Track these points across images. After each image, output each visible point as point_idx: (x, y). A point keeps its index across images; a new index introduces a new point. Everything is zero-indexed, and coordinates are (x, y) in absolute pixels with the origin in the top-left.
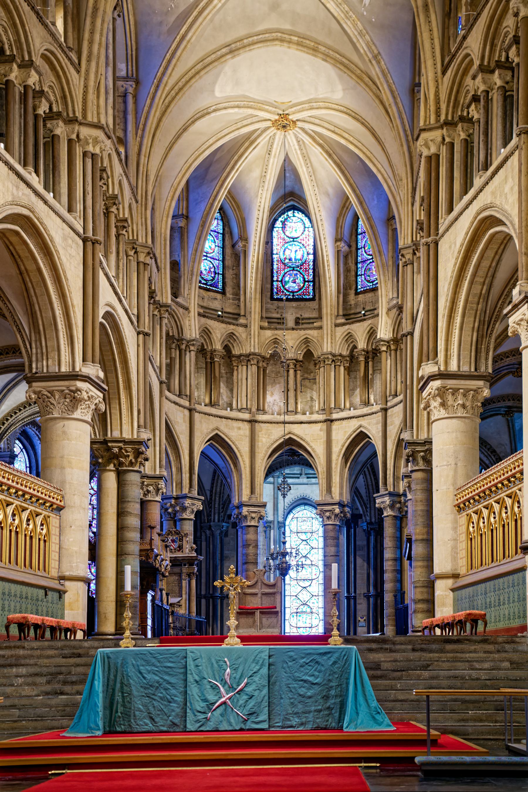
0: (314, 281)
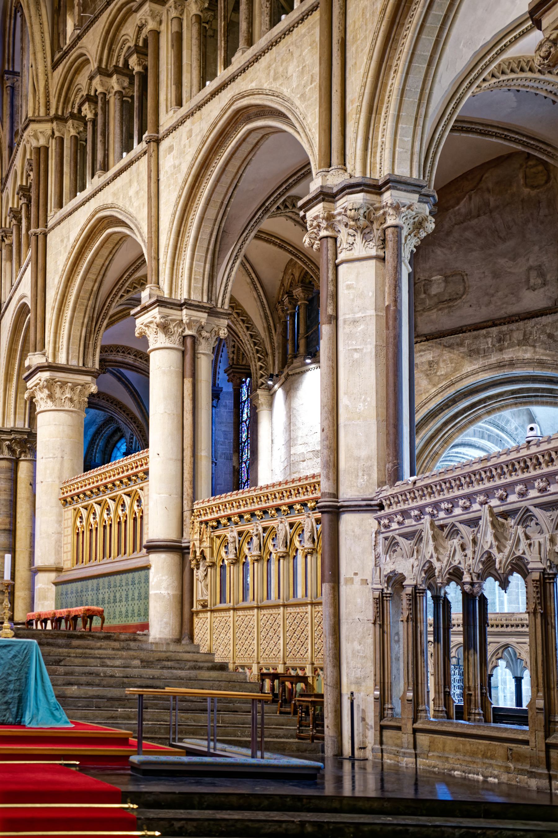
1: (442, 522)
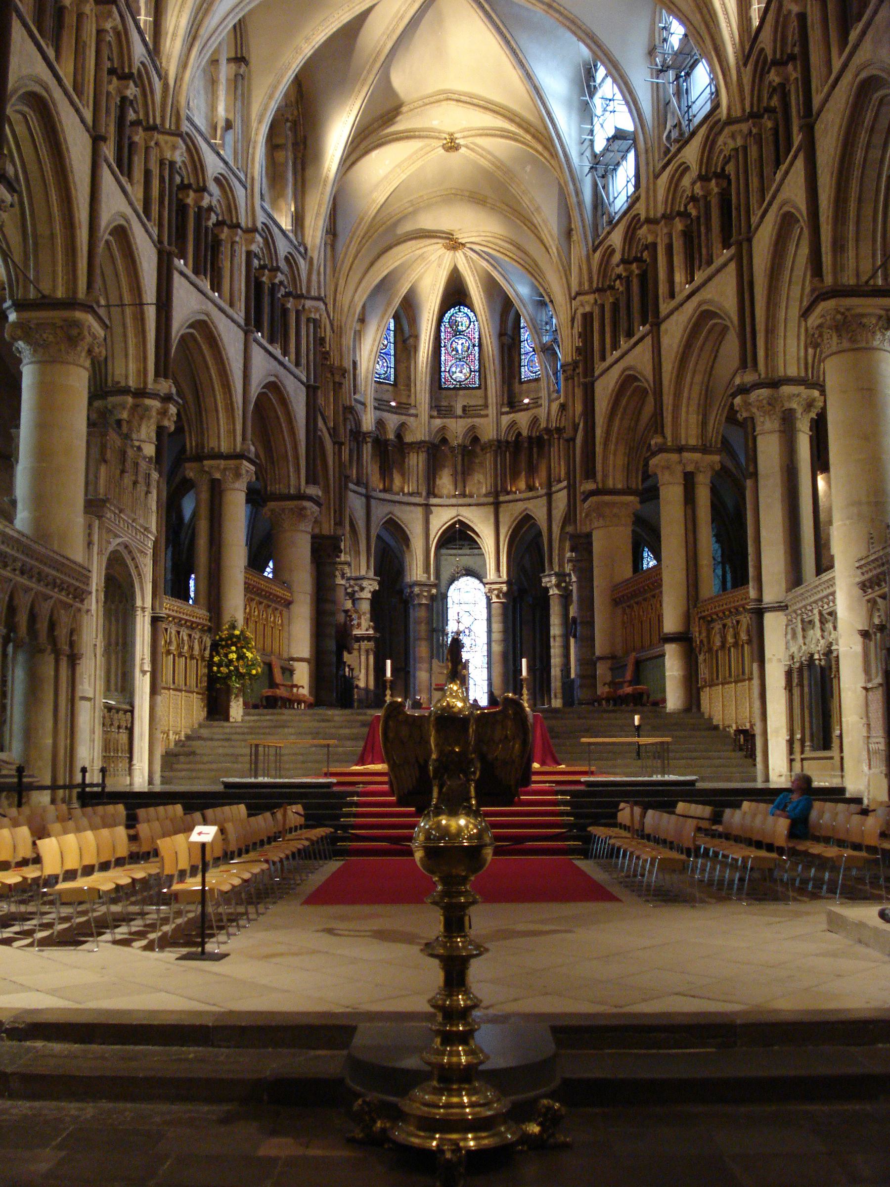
0: (479, 371)
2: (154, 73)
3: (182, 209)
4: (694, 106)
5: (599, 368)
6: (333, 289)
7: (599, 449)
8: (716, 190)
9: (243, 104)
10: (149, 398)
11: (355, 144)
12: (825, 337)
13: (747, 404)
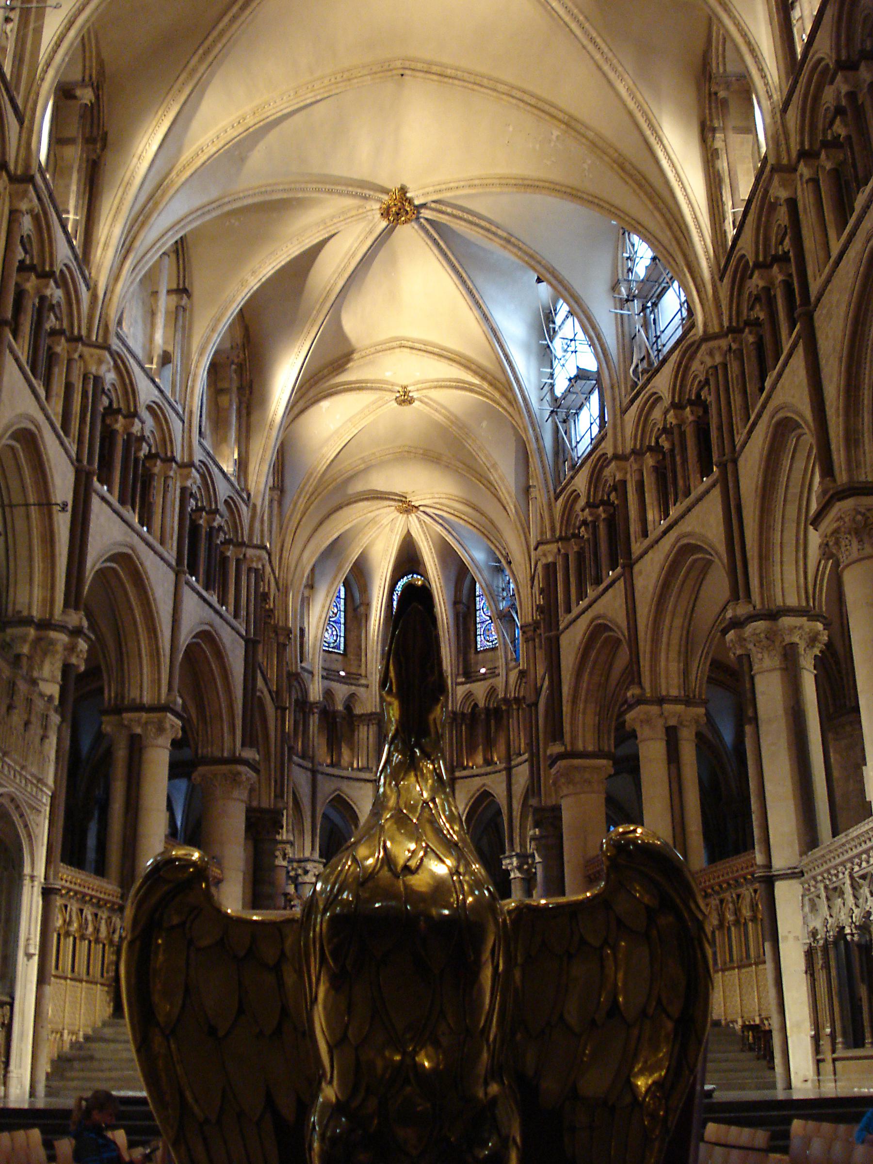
1: (835, 885)
2: (82, 281)
3: (109, 436)
4: (662, 336)
5: (564, 620)
6: (279, 545)
7: (566, 708)
8: (691, 418)
9: (183, 336)
10: (55, 630)
11: (303, 390)
12: (843, 543)
13: (742, 640)
